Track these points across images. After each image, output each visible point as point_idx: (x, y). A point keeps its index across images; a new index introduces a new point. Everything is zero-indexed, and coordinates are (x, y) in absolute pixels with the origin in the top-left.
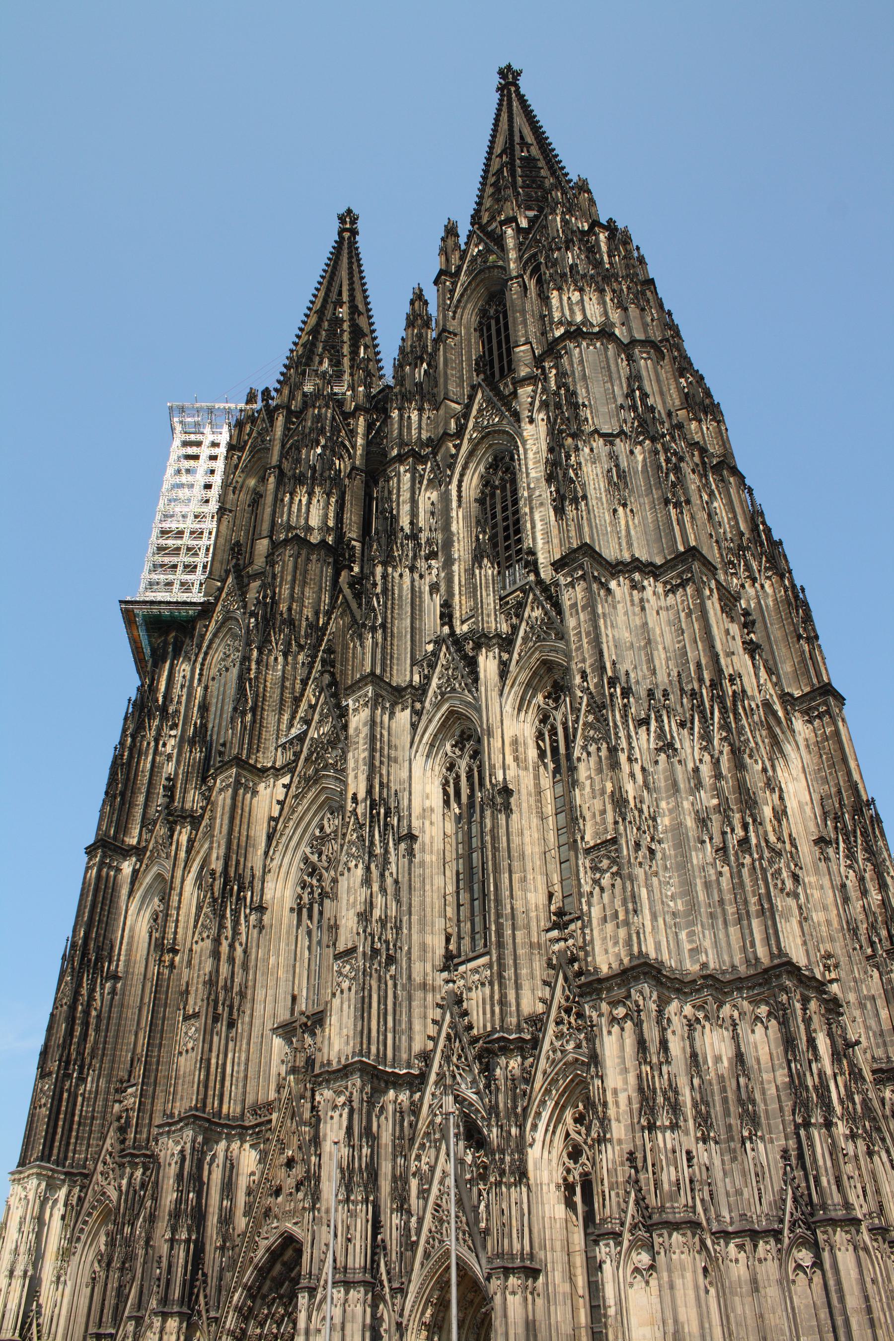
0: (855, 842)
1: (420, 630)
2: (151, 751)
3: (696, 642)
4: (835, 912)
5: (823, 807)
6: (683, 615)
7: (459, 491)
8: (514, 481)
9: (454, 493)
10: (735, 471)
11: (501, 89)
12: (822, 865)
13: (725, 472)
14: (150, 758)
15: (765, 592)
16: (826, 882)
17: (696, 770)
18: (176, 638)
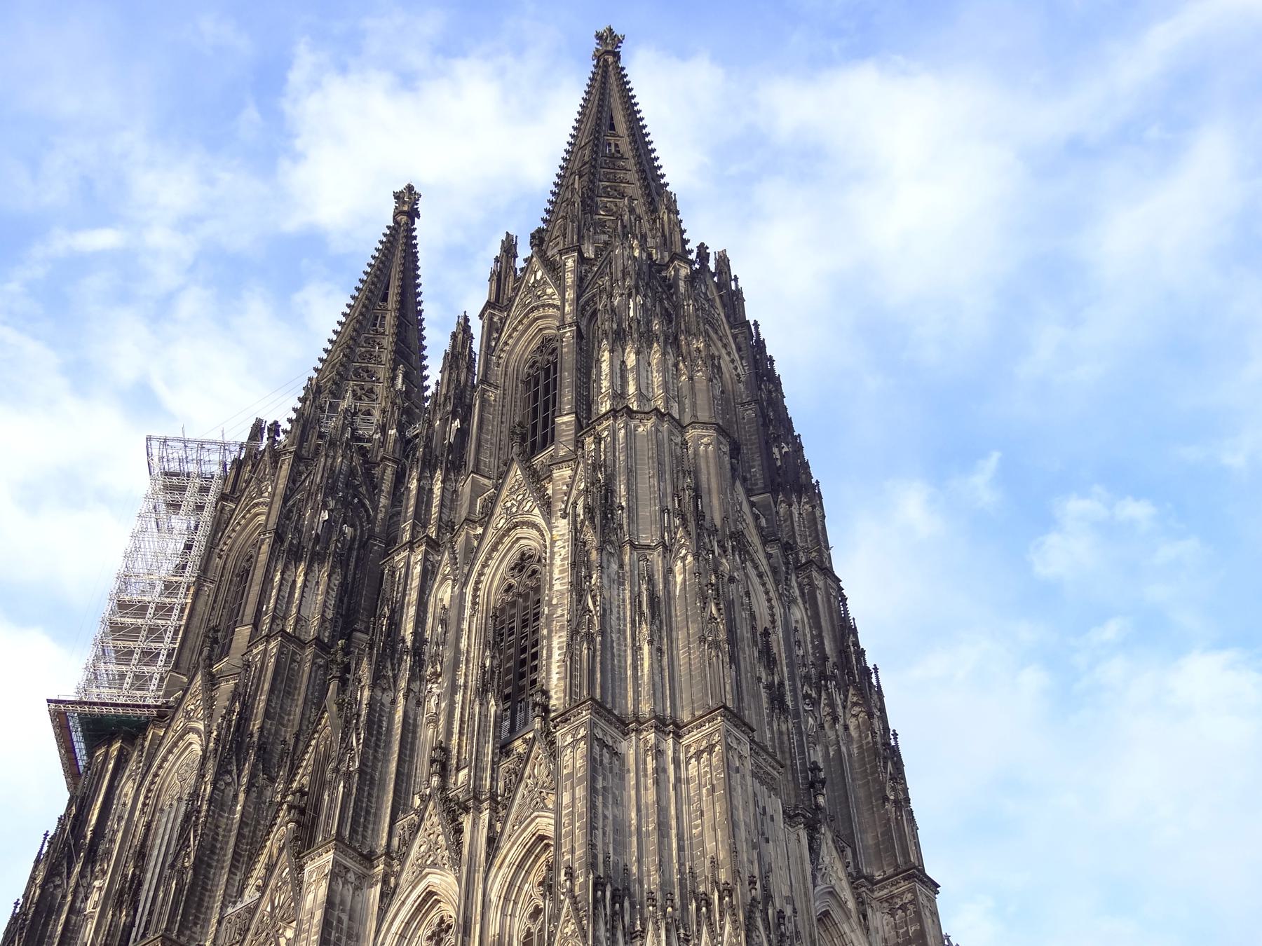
1: (409, 777)
2: (66, 908)
3: (715, 830)
6: (704, 790)
7: (475, 596)
8: (537, 590)
9: (469, 598)
10: (828, 572)
11: (598, 57)
13: (814, 574)
14: (63, 917)
15: (849, 735)
18: (121, 750)
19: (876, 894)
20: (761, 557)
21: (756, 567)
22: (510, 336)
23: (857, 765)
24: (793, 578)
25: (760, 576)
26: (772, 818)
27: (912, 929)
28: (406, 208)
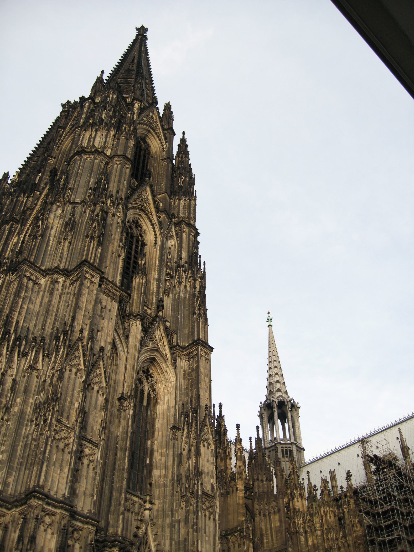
0: (191, 428)
4: (171, 470)
5: (183, 409)
12: (171, 442)
16: (171, 453)
17: (45, 381)
19: (184, 353)
20: (155, 219)
21: (151, 221)
22: (64, 138)
23: (187, 302)
24: (173, 228)
25: (152, 225)
26: (110, 310)
27: (195, 366)
28: (66, 109)
